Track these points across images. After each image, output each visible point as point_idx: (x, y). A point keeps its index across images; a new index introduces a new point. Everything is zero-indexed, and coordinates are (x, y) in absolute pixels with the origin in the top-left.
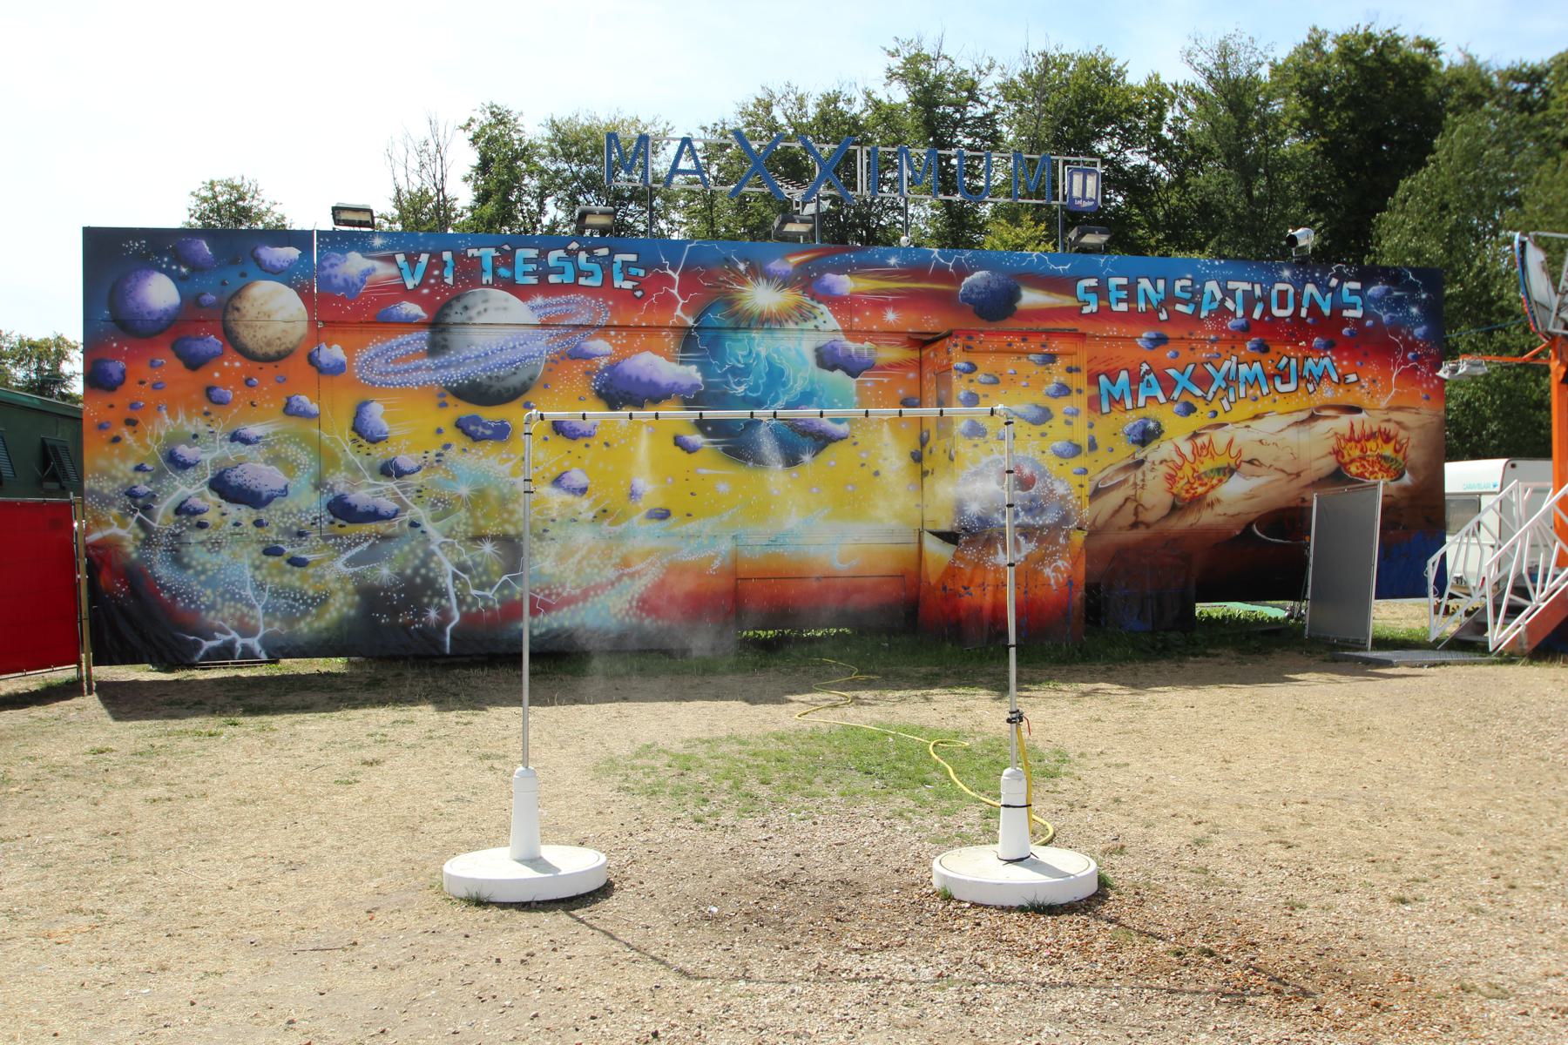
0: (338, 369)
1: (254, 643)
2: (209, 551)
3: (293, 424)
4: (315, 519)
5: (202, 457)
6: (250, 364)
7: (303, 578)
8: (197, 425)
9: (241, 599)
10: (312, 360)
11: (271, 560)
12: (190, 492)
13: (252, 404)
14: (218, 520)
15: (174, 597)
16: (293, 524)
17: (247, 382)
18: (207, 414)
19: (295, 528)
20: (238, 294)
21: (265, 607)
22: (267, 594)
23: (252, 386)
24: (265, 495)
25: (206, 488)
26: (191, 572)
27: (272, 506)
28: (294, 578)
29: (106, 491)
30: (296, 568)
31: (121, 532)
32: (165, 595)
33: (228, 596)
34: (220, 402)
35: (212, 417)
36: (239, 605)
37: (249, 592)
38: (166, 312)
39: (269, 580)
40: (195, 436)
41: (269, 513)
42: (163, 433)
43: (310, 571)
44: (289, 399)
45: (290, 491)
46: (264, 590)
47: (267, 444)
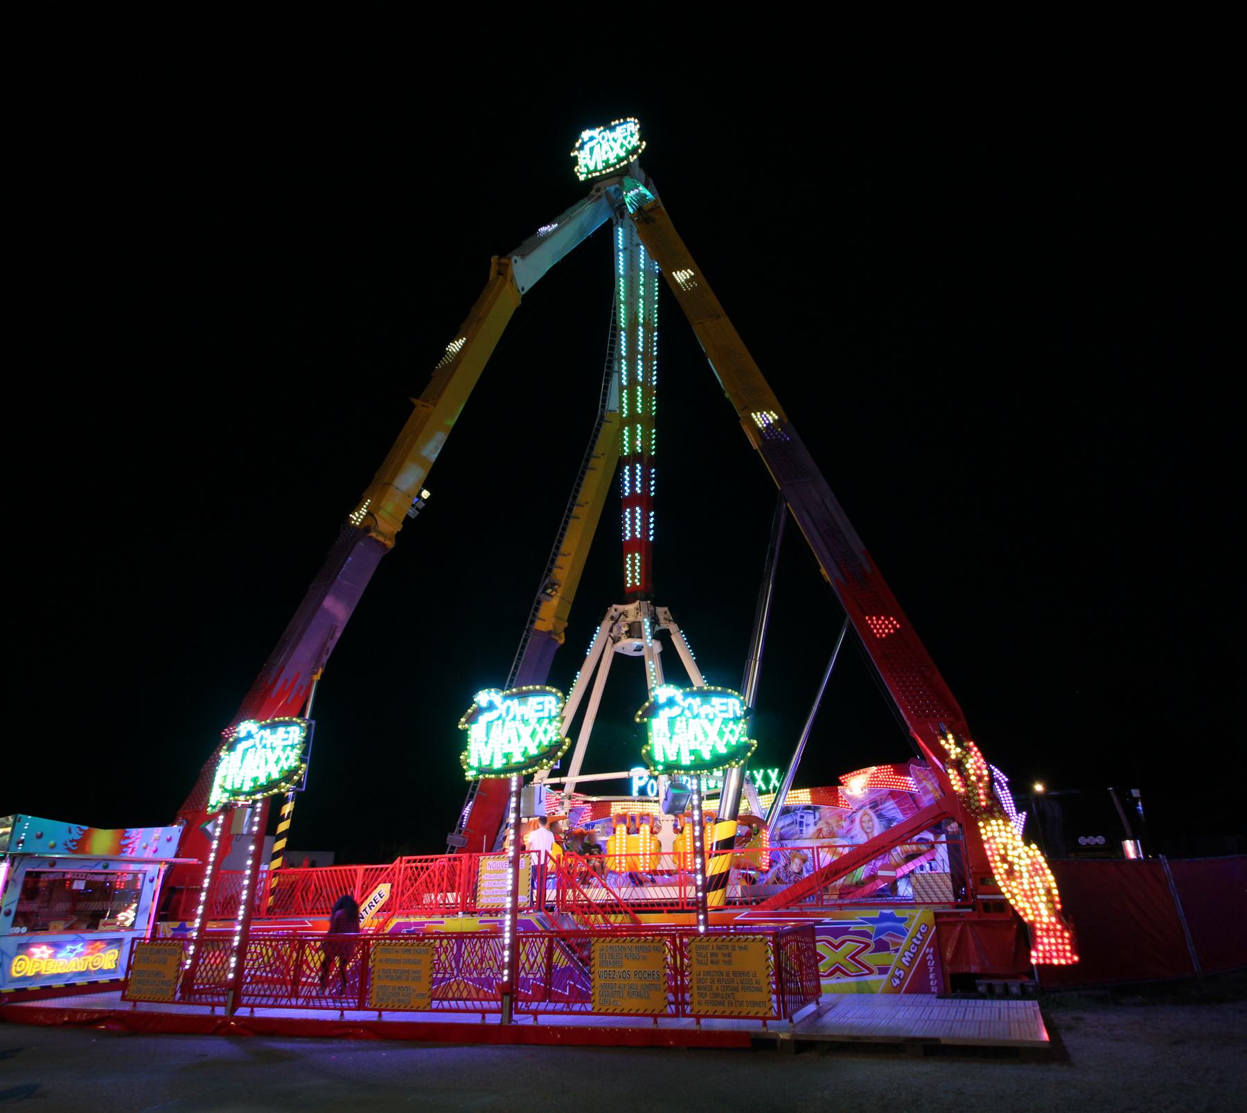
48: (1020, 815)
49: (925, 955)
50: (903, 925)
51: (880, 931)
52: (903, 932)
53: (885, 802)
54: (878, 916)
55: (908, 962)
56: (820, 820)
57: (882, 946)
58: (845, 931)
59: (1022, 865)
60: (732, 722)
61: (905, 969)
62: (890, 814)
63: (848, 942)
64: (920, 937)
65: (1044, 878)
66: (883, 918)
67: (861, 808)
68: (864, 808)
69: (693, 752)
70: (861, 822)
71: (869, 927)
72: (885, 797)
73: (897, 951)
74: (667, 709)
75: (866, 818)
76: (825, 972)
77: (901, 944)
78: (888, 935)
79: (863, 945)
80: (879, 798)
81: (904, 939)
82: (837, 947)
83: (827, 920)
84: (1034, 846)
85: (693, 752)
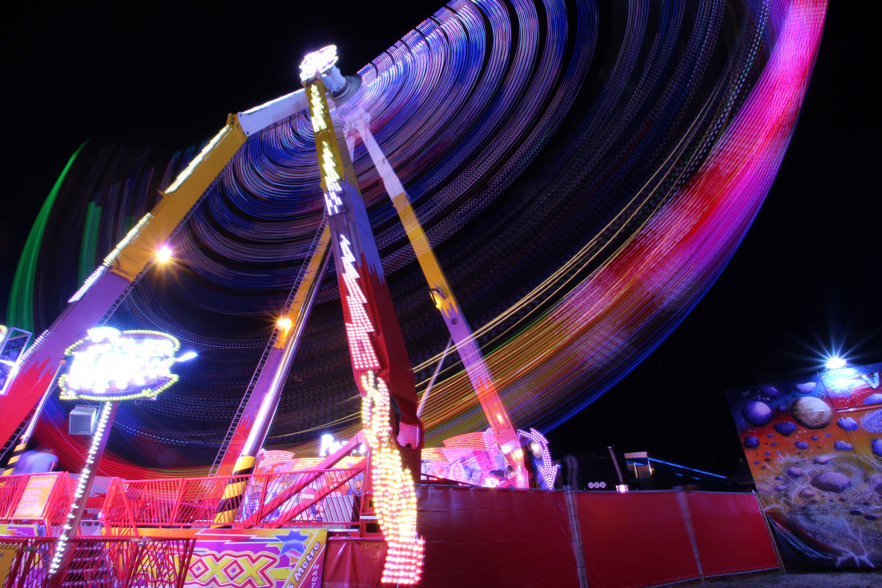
0: (854, 427)
1: (864, 558)
2: (822, 513)
3: (841, 454)
4: (871, 496)
5: (804, 472)
6: (810, 431)
7: (877, 526)
8: (795, 459)
9: (848, 537)
10: (840, 425)
11: (855, 517)
13: (818, 447)
14: (821, 499)
15: (814, 535)
16: (860, 499)
17: (812, 438)
18: (799, 453)
19: (862, 501)
20: (795, 403)
21: (863, 541)
22: (861, 534)
23: (815, 440)
24: (840, 487)
25: (810, 485)
26: (817, 523)
27: (845, 491)
28: (871, 525)
29: (766, 489)
30: (871, 521)
31: (778, 506)
32: (809, 534)
33: (841, 535)
34: (803, 448)
35: (802, 454)
36: (849, 540)
37: (851, 533)
38: (767, 415)
39: (859, 527)
40: (797, 463)
41: (847, 494)
42: (782, 463)
43: (880, 522)
44: (835, 443)
45: (853, 484)
46: (858, 532)
47: (832, 463)
49: (313, 571)
50: (303, 543)
51: (287, 548)
52: (301, 549)
53: (470, 458)
54: (287, 534)
55: (299, 577)
56: (429, 470)
57: (285, 562)
58: (263, 547)
59: (395, 489)
60: (159, 359)
61: (296, 584)
62: (471, 466)
63: (263, 557)
64: (312, 554)
65: (408, 500)
66: (293, 536)
67: (454, 462)
70: (454, 471)
71: (280, 545)
73: (293, 566)
74: (98, 345)
75: (457, 469)
76: (240, 584)
77: (297, 560)
78: (291, 552)
79: (272, 560)
80: (466, 455)
81: (301, 555)
82: (254, 561)
83: (253, 537)
84: (408, 471)
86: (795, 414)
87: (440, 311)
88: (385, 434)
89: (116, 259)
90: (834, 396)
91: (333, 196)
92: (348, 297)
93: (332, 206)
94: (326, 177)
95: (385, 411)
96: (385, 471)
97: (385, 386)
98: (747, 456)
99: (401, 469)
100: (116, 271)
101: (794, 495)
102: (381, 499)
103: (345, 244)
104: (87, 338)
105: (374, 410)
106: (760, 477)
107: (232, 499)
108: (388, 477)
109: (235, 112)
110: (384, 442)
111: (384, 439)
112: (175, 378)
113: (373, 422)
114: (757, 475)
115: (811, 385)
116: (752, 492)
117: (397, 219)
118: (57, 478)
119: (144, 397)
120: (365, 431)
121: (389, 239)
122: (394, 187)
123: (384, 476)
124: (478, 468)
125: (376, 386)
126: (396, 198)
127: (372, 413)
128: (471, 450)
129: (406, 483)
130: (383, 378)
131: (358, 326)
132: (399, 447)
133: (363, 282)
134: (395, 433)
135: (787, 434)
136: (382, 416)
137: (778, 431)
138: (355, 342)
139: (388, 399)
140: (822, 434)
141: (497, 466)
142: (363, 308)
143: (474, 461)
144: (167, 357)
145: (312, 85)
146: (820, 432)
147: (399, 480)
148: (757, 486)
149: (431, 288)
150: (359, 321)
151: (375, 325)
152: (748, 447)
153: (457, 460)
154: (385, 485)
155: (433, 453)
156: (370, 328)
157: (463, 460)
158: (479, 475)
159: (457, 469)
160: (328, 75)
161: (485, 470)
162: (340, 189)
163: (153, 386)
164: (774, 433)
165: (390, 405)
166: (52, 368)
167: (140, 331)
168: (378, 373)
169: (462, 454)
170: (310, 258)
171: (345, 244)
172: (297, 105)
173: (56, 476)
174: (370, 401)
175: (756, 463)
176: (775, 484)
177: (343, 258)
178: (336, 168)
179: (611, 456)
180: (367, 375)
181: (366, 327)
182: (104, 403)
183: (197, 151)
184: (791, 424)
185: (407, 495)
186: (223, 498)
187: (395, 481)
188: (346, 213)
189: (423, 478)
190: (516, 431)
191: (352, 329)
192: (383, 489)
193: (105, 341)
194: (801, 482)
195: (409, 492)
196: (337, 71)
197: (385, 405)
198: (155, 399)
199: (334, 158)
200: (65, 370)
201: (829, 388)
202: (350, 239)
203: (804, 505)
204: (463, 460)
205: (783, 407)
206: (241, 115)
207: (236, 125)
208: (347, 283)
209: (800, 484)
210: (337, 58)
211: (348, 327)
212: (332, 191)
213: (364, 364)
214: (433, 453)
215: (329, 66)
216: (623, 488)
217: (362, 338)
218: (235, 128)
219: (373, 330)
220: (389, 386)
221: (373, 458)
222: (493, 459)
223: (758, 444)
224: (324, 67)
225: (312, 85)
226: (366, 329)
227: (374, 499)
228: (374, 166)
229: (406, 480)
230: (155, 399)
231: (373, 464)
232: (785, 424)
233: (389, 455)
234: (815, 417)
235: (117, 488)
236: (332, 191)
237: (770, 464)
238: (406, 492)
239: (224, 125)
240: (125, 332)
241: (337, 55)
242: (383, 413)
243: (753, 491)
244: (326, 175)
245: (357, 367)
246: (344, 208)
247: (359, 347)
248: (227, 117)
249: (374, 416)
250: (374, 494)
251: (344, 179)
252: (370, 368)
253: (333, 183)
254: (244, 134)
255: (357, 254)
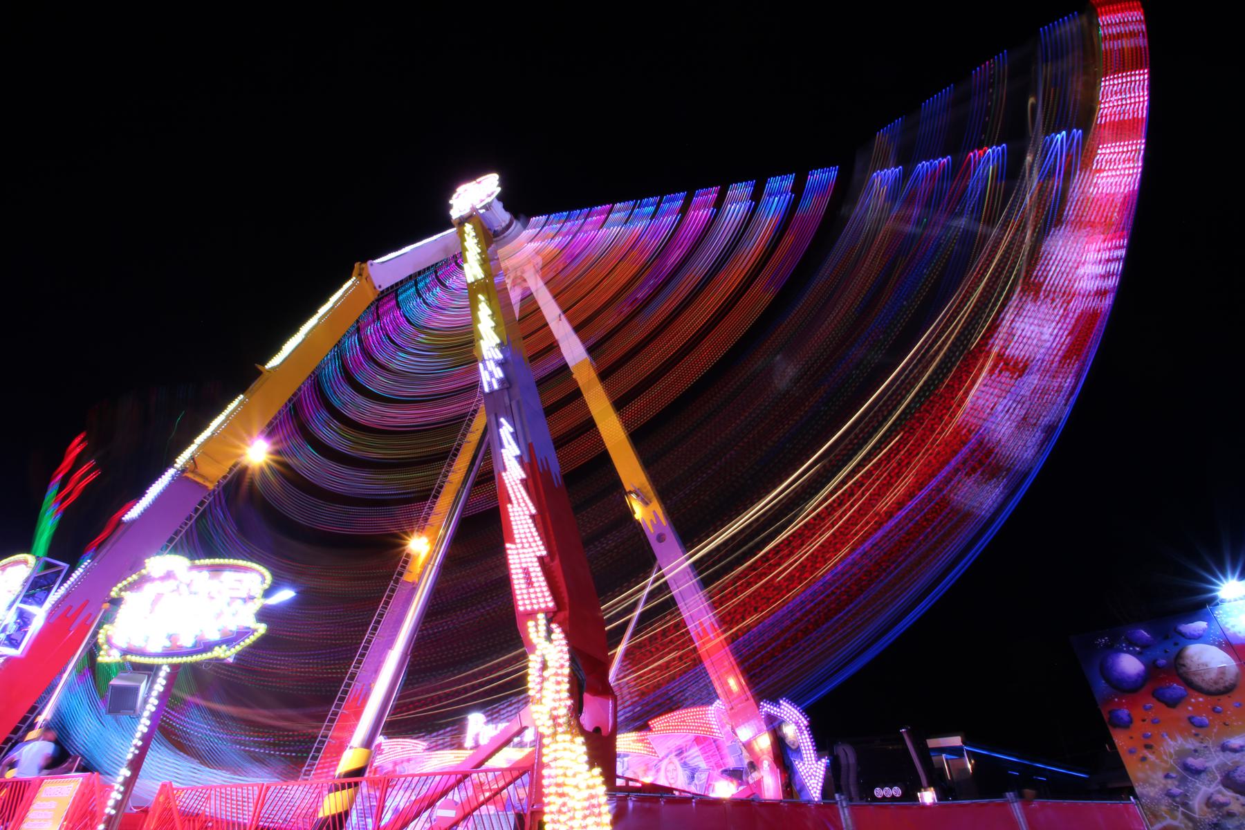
5: (1207, 764)
8: (1191, 744)
12: (1211, 790)
13: (1225, 724)
18: (1196, 735)
20: (1179, 655)
23: (1219, 712)
25: (1221, 787)
29: (1152, 794)
31: (1175, 823)
34: (1201, 726)
35: (1201, 737)
38: (1138, 675)
40: (1196, 751)
42: (1172, 751)
48: (819, 763)
53: (690, 748)
56: (628, 769)
60: (240, 602)
67: (667, 756)
68: (670, 756)
69: (170, 637)
70: (666, 771)
72: (690, 742)
74: (158, 583)
80: (684, 745)
84: (597, 770)
85: (170, 637)
86: (1181, 671)
87: (640, 524)
88: (563, 711)
89: (192, 458)
90: (1238, 642)
91: (491, 365)
92: (509, 506)
93: (489, 379)
94: (481, 341)
95: (562, 675)
96: (560, 772)
97: (562, 636)
98: (1116, 741)
99: (587, 767)
100: (190, 475)
101: (1197, 803)
102: (555, 817)
103: (506, 430)
104: (144, 572)
105: (546, 674)
106: (1140, 775)
107: (333, 817)
108: (567, 781)
109: (364, 261)
110: (560, 725)
111: (560, 721)
112: (262, 629)
113: (544, 692)
114: (1135, 771)
115: (1200, 625)
116: (1130, 800)
117: (577, 394)
118: (82, 784)
119: (217, 659)
120: (532, 707)
121: (565, 421)
122: (573, 350)
123: (560, 780)
124: (703, 765)
125: (549, 638)
126: (577, 365)
127: (544, 679)
128: (691, 736)
129: (593, 792)
130: (560, 625)
131: (523, 548)
132: (583, 732)
133: (530, 483)
134: (577, 710)
135: (1173, 703)
136: (558, 683)
137: (1159, 699)
138: (520, 571)
139: (567, 656)
140: (1226, 702)
141: (731, 763)
142: (530, 521)
143: (696, 754)
144: (252, 598)
145: (466, 224)
146: (1224, 698)
147: (583, 785)
148: (1138, 790)
149: (627, 490)
150: (524, 541)
151: (547, 544)
152: (1115, 726)
153: (671, 752)
154: (562, 795)
155: (634, 741)
156: (540, 550)
157: (680, 752)
158: (704, 776)
159: (671, 767)
160: (487, 210)
161: (713, 769)
162: (500, 356)
163: (229, 641)
164: (1152, 703)
165: (570, 666)
166: (91, 614)
167: (217, 561)
168: (551, 617)
169: (679, 742)
170: (458, 450)
171: (506, 430)
172: (446, 249)
173: (81, 779)
174: (539, 660)
175: (1131, 752)
176: (1165, 785)
177: (503, 451)
178: (496, 329)
179: (906, 744)
180: (536, 620)
181: (536, 549)
182: (159, 667)
183: (313, 311)
184: (1177, 688)
185: (596, 811)
186: (321, 815)
187: (576, 786)
188: (507, 388)
189: (619, 782)
190: (758, 705)
191: (515, 552)
192: (560, 801)
193: (169, 576)
194: (1206, 782)
195: (599, 805)
196: (499, 206)
197: (562, 666)
198: (231, 660)
199: (493, 316)
200: (108, 618)
201: (1228, 629)
202: (513, 425)
203: (1215, 820)
204: (680, 752)
205: (1162, 662)
206: (372, 265)
207: (364, 277)
208: (508, 485)
209: (1203, 784)
210: (499, 189)
211: (510, 549)
212: (489, 359)
213: (532, 604)
214: (634, 741)
215: (489, 200)
216: (928, 797)
217: (530, 565)
218: (364, 280)
219: (544, 553)
220: (569, 636)
221: (545, 751)
222: (726, 751)
223: (1131, 721)
224: (482, 201)
225: (466, 224)
226: (534, 552)
227: (546, 818)
228: (547, 324)
229: (593, 787)
230: (231, 660)
231: (545, 760)
232: (1169, 688)
233: (568, 745)
234: (1213, 675)
235: (167, 798)
236: (489, 359)
237: (1154, 752)
238: (593, 806)
239: (349, 277)
240: (197, 562)
241: (499, 186)
242: (559, 679)
243: (1131, 797)
244: (481, 338)
245: (521, 608)
246: (506, 382)
247: (524, 578)
248: (353, 268)
249: (545, 684)
250: (546, 809)
251: (506, 343)
252: (540, 610)
253: (491, 349)
254: (375, 288)
255: (523, 445)
